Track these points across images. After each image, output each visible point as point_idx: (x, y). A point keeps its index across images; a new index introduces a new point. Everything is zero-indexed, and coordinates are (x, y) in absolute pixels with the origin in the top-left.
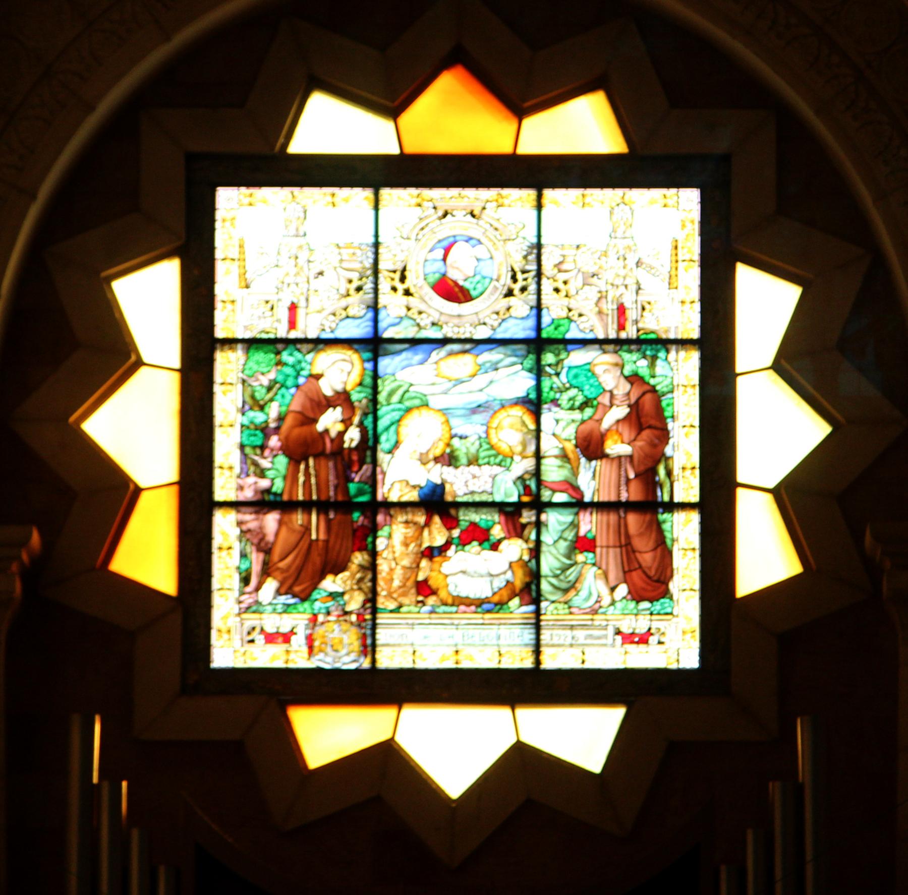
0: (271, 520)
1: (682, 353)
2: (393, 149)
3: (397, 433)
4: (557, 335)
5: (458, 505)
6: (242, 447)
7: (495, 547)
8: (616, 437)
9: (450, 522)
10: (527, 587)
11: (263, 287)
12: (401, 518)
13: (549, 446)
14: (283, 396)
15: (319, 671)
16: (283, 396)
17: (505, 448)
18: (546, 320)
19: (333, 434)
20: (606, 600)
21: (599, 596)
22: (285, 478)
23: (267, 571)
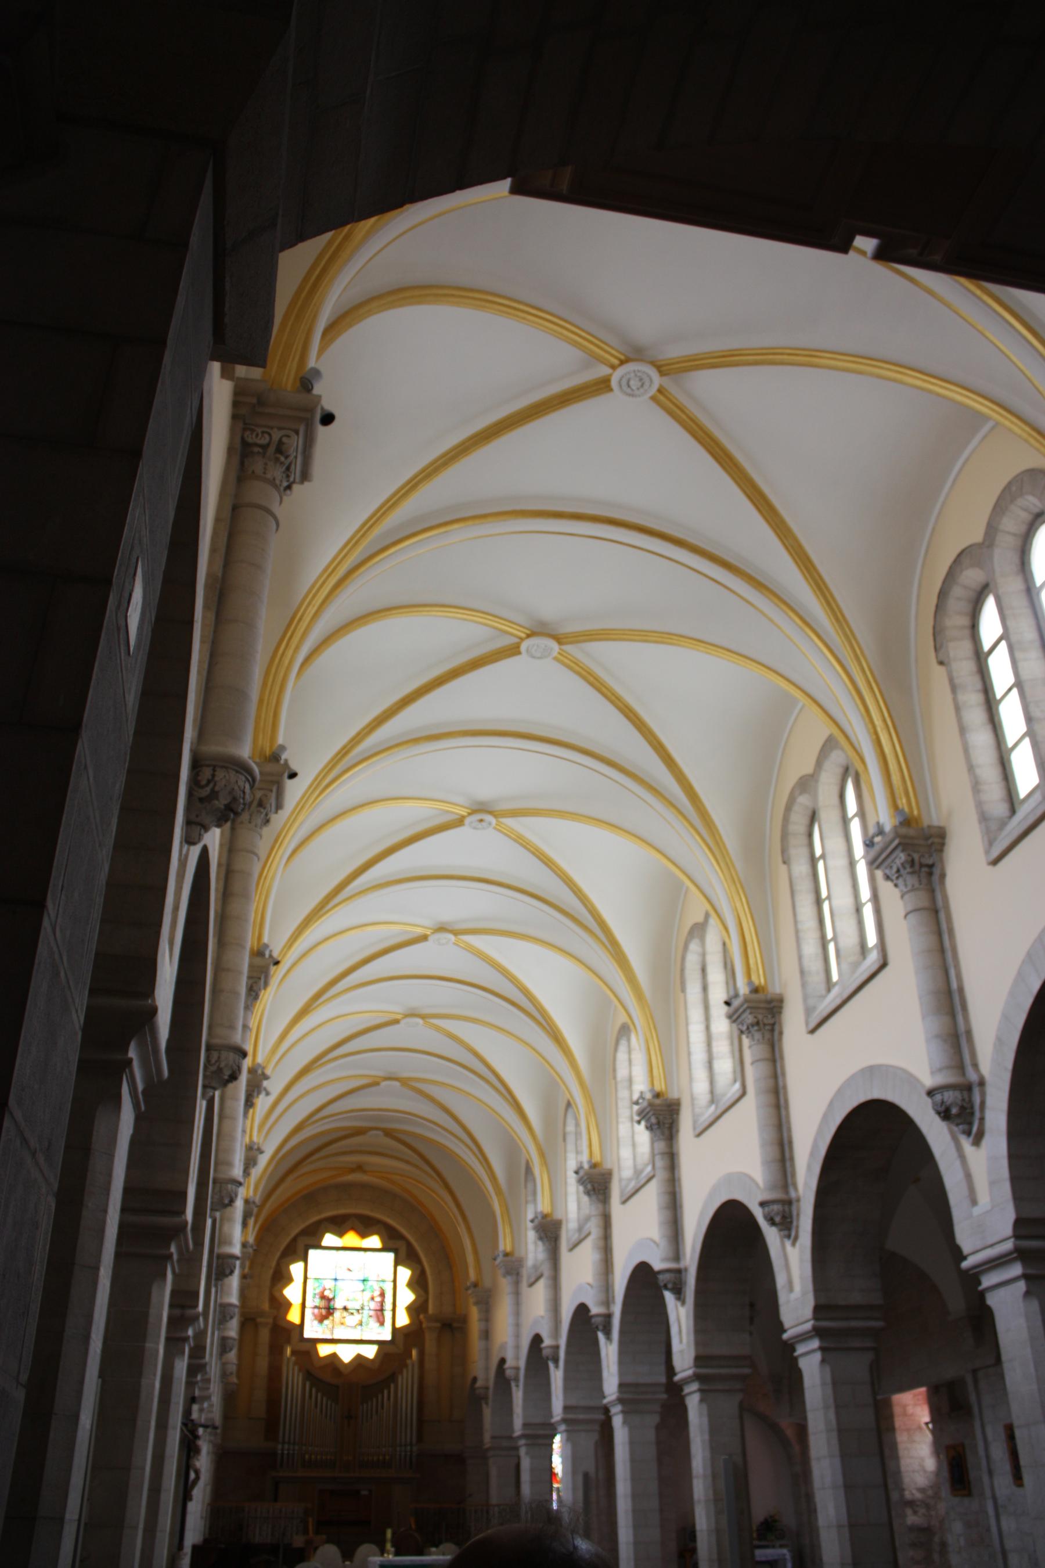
0: (316, 1311)
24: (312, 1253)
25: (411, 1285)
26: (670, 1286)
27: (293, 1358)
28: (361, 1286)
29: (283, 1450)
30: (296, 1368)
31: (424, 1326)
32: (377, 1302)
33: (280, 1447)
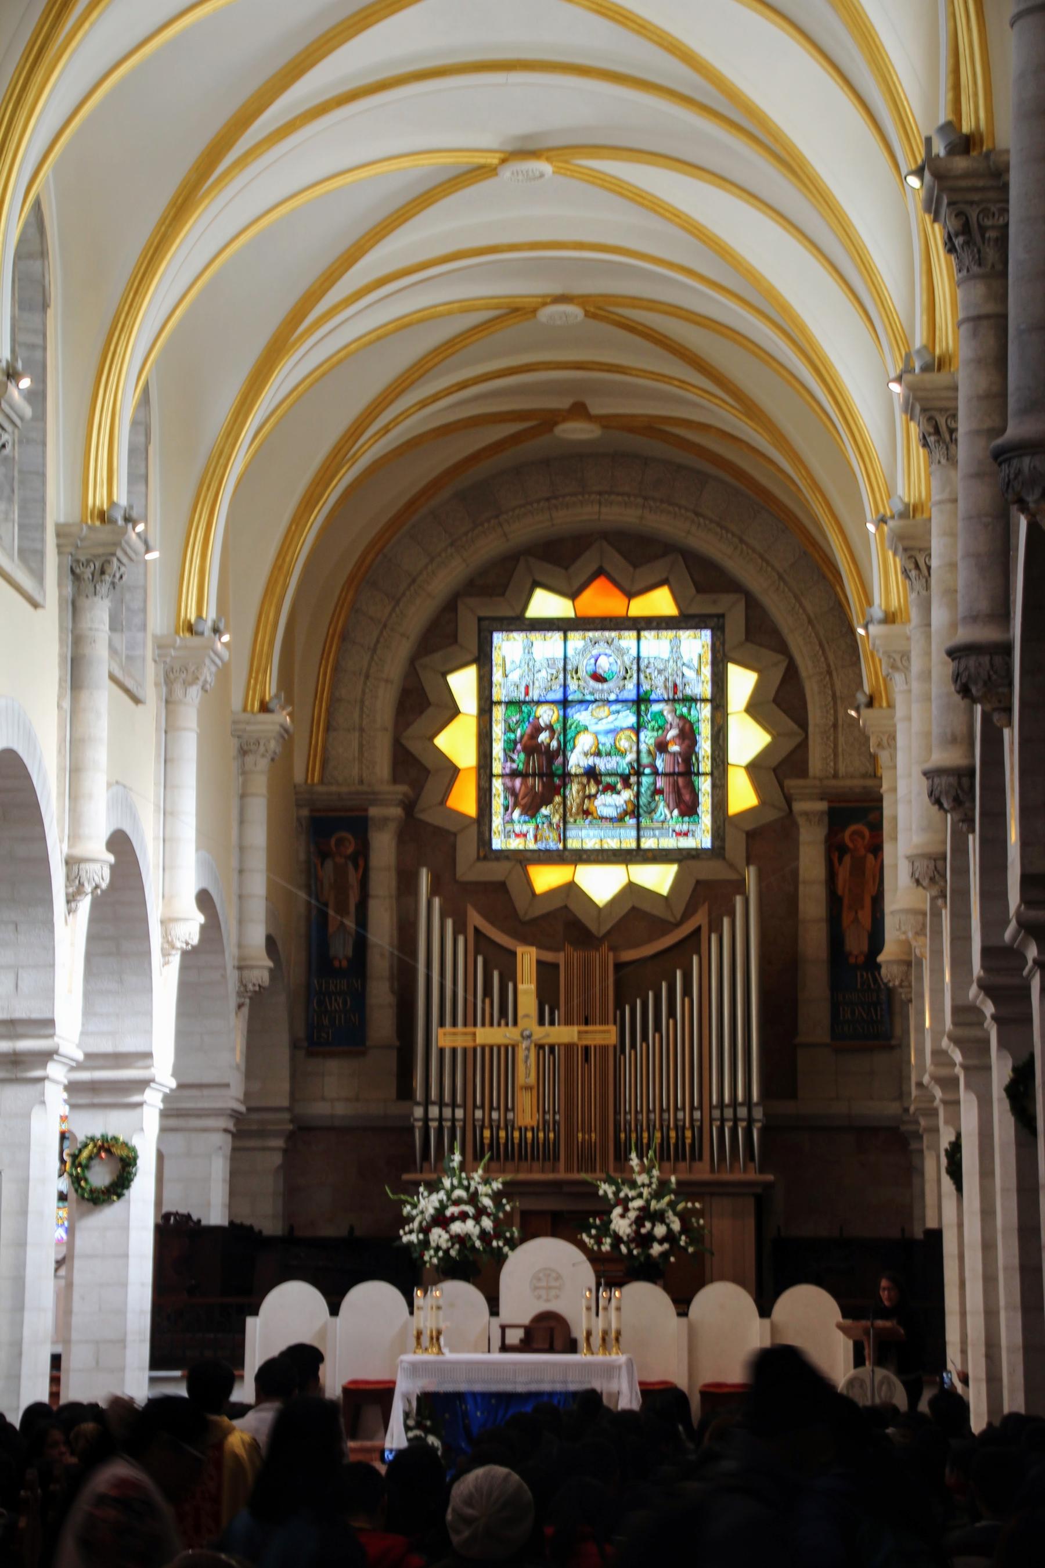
0: (518, 782)
1: (703, 704)
2: (572, 615)
3: (574, 742)
4: (647, 697)
5: (601, 775)
6: (505, 750)
7: (619, 793)
8: (672, 742)
9: (598, 782)
10: (633, 812)
11: (514, 677)
12: (576, 780)
13: (643, 747)
14: (523, 727)
15: (540, 850)
16: (523, 727)
17: (622, 749)
18: (641, 690)
19: (545, 743)
20: (669, 816)
21: (665, 814)
22: (524, 764)
23: (516, 805)
29: (426, 1119)
30: (449, 923)
31: (798, 806)
32: (674, 754)
33: (419, 1112)
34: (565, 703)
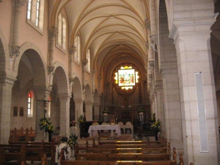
24: (119, 71)
25: (138, 75)
26: (151, 65)
27: (115, 90)
28: (129, 76)
31: (141, 82)
34: (124, 75)
